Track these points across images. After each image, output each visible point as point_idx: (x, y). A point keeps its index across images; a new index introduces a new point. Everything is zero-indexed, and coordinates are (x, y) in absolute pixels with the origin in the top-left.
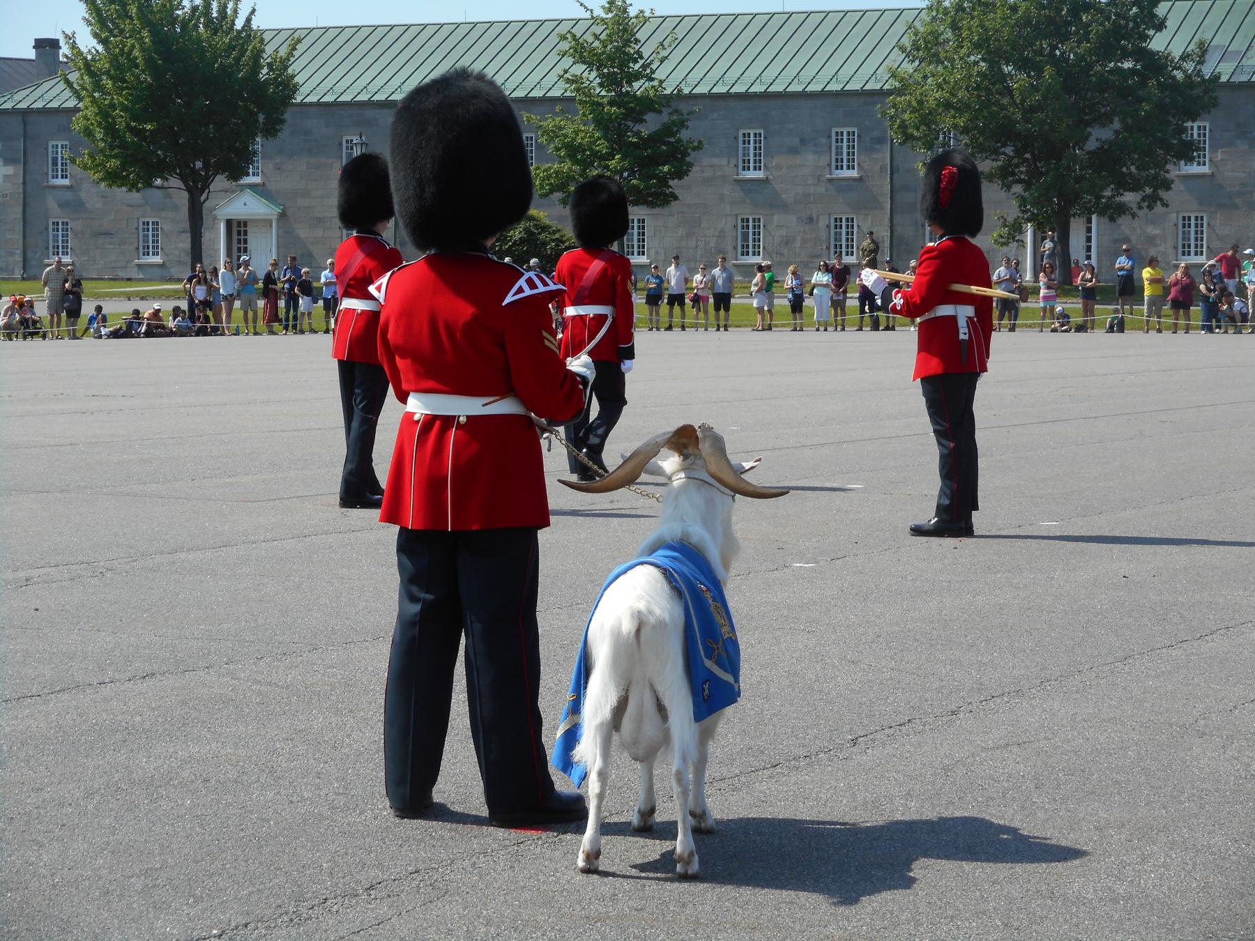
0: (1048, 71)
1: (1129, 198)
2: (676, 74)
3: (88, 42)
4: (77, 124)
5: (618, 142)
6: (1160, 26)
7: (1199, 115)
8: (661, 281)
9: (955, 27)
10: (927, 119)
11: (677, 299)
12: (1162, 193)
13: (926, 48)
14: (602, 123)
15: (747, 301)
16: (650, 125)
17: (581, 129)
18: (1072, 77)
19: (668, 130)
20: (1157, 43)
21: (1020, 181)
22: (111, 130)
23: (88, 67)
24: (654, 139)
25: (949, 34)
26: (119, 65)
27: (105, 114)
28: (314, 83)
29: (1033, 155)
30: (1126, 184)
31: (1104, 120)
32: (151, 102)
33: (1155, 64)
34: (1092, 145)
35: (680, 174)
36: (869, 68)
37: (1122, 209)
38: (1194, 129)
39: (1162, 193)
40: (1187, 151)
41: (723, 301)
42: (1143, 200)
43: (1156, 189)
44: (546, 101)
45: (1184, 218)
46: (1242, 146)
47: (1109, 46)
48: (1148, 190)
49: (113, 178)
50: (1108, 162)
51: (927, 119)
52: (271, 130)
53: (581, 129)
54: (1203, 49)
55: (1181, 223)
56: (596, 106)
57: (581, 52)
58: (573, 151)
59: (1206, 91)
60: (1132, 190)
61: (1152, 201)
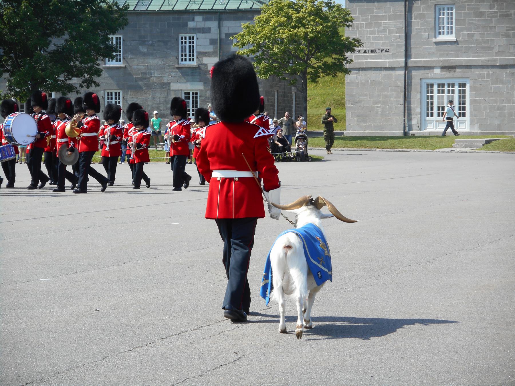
7: (117, 30)
12: (95, 78)
21: (7, 71)
29: (15, 55)
30: (71, 73)
31: (59, 33)
34: (52, 48)
38: (114, 38)
39: (95, 78)
40: (109, 52)
42: (84, 82)
43: (91, 75)
45: (108, 94)
46: (143, 49)
48: (87, 76)
50: (61, 58)
55: (106, 96)
59: (121, 16)
60: (77, 76)
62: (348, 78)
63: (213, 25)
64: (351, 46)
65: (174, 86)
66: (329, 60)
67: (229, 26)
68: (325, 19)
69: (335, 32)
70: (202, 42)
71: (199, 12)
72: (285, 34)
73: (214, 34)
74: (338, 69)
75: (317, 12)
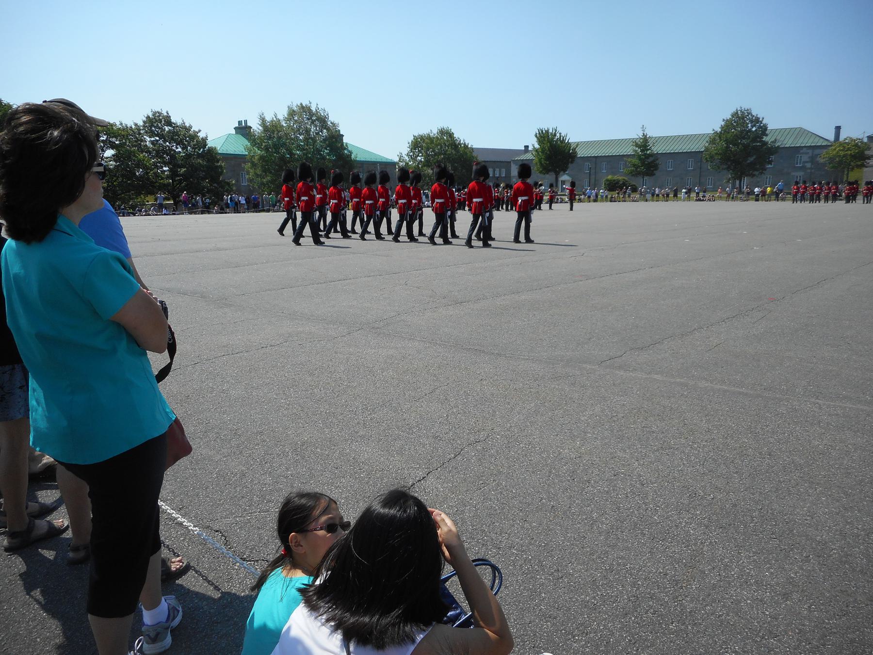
0: (740, 146)
1: (756, 173)
2: (657, 149)
3: (537, 146)
4: (534, 162)
5: (643, 164)
6: (767, 135)
8: (654, 191)
9: (720, 137)
10: (712, 157)
11: (658, 195)
13: (712, 141)
14: (640, 159)
15: (671, 195)
16: (651, 159)
17: (636, 161)
18: (746, 147)
19: (654, 161)
20: (765, 139)
22: (541, 163)
23: (537, 151)
24: (653, 162)
25: (717, 138)
26: (543, 152)
27: (540, 160)
28: (581, 153)
30: (756, 170)
32: (549, 158)
33: (765, 143)
35: (656, 169)
36: (699, 146)
37: (753, 176)
40: (770, 162)
41: (668, 195)
44: (628, 156)
47: (754, 140)
49: (541, 172)
51: (712, 157)
52: (572, 162)
53: (636, 161)
54: (776, 140)
56: (639, 156)
57: (637, 145)
58: (634, 165)
61: (762, 173)
62: (865, 169)
63: (810, 151)
64: (869, 158)
65: (793, 174)
66: (859, 163)
67: (817, 151)
68: (859, 147)
69: (863, 152)
70: (805, 158)
71: (805, 147)
72: (842, 153)
73: (810, 154)
74: (863, 166)
75: (856, 145)
